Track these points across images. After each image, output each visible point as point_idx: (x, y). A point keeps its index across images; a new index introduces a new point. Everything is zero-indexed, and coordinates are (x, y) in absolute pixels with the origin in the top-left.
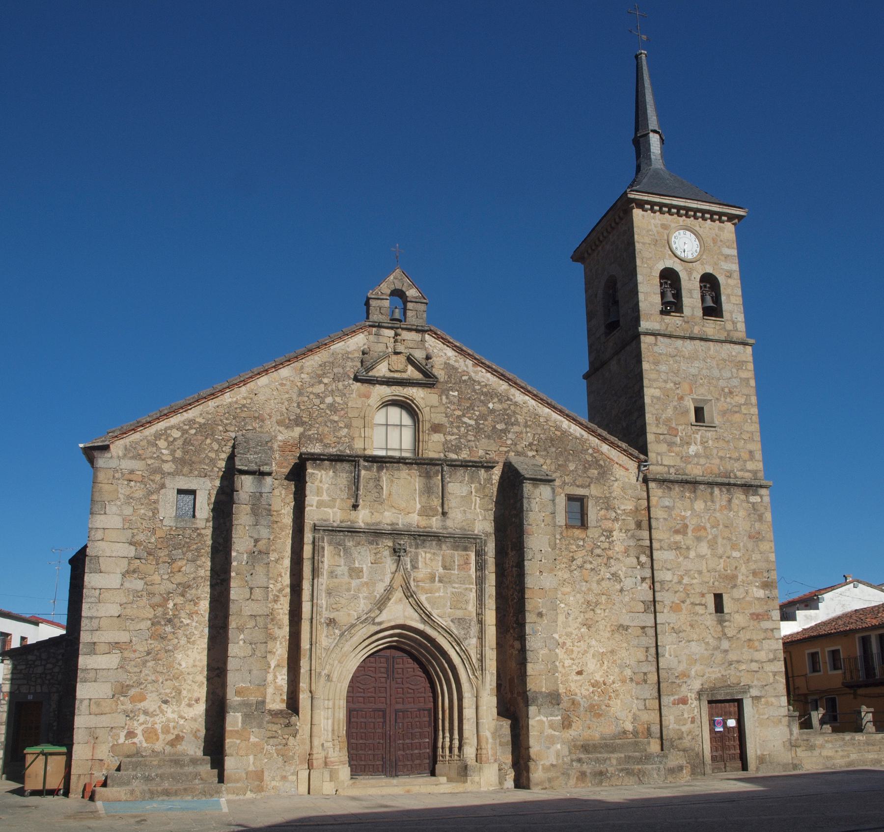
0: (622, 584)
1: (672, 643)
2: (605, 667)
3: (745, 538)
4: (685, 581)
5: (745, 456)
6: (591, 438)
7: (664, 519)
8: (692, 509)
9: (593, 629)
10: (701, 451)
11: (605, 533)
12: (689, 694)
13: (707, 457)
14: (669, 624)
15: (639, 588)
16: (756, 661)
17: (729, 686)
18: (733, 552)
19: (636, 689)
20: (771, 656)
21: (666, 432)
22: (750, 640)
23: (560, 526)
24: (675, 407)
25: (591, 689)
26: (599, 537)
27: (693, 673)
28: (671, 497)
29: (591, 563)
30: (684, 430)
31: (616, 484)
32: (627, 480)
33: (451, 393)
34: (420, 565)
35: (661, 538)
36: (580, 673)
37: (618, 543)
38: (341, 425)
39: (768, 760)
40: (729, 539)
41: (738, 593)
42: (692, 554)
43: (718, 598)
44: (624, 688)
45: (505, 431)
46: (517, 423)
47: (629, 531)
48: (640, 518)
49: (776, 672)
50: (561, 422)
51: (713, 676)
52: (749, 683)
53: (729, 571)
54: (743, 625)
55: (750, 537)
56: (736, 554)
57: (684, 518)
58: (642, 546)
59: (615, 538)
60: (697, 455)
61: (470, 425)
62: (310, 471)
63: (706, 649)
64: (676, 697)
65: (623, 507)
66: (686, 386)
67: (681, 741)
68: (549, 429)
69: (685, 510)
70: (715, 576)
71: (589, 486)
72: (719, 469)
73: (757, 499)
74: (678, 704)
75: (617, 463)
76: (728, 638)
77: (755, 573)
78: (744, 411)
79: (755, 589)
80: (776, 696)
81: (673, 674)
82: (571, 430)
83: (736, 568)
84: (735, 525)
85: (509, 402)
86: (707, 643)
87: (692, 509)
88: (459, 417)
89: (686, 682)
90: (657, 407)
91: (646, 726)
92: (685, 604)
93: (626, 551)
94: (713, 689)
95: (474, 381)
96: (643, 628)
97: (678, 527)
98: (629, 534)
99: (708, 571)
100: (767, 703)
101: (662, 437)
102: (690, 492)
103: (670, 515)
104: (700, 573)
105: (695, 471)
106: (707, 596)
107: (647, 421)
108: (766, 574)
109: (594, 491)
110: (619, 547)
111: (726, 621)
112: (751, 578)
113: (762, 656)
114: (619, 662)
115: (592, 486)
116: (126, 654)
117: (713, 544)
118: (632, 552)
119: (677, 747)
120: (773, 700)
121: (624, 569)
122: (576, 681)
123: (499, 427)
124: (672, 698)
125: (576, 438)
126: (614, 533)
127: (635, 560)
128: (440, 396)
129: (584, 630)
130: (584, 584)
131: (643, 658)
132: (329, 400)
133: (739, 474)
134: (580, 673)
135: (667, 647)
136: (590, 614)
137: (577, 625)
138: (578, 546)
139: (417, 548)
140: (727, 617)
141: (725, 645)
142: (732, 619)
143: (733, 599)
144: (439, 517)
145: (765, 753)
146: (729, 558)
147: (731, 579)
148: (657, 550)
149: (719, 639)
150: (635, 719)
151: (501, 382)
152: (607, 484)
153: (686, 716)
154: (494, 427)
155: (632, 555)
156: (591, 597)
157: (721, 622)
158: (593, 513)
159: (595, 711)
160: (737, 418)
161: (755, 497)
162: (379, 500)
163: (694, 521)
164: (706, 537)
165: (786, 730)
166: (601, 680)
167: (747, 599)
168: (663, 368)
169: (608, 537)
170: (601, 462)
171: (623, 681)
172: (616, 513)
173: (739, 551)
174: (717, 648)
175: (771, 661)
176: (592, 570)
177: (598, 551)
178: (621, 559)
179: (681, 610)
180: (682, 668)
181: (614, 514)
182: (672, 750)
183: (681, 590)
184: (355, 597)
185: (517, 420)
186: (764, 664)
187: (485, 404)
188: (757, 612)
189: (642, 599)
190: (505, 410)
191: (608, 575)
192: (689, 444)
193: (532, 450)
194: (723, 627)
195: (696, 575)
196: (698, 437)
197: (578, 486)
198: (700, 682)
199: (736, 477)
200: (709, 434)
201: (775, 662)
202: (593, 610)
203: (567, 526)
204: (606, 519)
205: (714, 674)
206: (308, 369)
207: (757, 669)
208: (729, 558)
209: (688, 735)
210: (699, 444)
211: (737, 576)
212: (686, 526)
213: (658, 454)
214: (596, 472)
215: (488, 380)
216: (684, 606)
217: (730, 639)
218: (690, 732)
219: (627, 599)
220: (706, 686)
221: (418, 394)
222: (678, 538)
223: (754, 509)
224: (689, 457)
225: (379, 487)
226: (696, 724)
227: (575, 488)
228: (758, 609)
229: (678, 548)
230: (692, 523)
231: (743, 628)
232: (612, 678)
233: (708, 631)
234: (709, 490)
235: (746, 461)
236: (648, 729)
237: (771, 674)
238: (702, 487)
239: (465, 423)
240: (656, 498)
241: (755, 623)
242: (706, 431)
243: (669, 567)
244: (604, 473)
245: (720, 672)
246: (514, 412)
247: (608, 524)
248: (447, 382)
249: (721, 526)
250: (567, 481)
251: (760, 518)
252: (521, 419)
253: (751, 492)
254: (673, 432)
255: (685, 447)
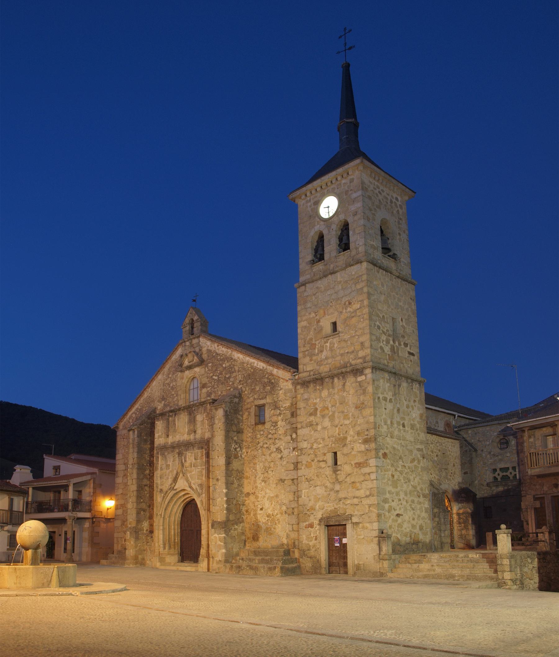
0: (282, 454)
1: (306, 489)
2: (273, 506)
3: (353, 409)
4: (314, 447)
5: (358, 347)
6: (268, 367)
7: (305, 408)
8: (321, 397)
9: (267, 483)
10: (329, 354)
11: (273, 424)
12: (315, 521)
13: (333, 357)
14: (304, 476)
15: (292, 455)
16: (357, 497)
17: (339, 515)
18: (345, 421)
19: (288, 518)
20: (368, 493)
21: (309, 349)
22: (353, 482)
23: (253, 425)
24: (315, 329)
25: (267, 519)
26: (271, 427)
27: (317, 507)
28: (308, 392)
29: (266, 443)
30: (319, 343)
31: (281, 392)
32: (287, 387)
33: (209, 365)
34: (187, 459)
35: (302, 421)
36: (261, 509)
37: (281, 428)
38: (175, 395)
39: (362, 568)
40: (343, 412)
41: (346, 450)
42: (319, 427)
43: (335, 453)
44: (282, 518)
45: (229, 378)
46: (235, 371)
47: (287, 419)
48: (293, 410)
49: (371, 505)
50: (254, 363)
51: (329, 509)
52: (352, 513)
53: (341, 435)
54: (349, 472)
55: (356, 408)
56: (347, 422)
57: (315, 404)
58: (293, 428)
59: (279, 426)
60: (327, 358)
61: (216, 380)
62: (156, 422)
63: (325, 491)
64: (307, 523)
65: (284, 406)
66: (321, 312)
67: (309, 551)
68: (248, 369)
69: (316, 399)
70: (333, 440)
71: (266, 397)
72: (340, 363)
73: (363, 377)
74: (308, 528)
75: (282, 378)
76: (339, 482)
77: (358, 434)
78: (358, 314)
79: (358, 445)
80: (370, 522)
81: (306, 508)
82: (258, 367)
83: (346, 432)
84: (346, 401)
85: (231, 361)
86: (326, 487)
87: (321, 397)
88: (212, 376)
89: (313, 513)
90: (305, 333)
91: (293, 541)
92: (315, 461)
93: (285, 434)
94: (328, 518)
95: (218, 354)
96: (293, 480)
97: (311, 411)
98: (287, 422)
99: (329, 438)
100: (363, 527)
101: (307, 353)
102: (320, 386)
103: (307, 405)
104: (323, 439)
105: (324, 369)
106: (327, 454)
107: (299, 345)
108: (366, 433)
109: (269, 400)
110: (281, 431)
111: (338, 471)
112: (356, 437)
113: (361, 493)
114: (280, 502)
115: (267, 397)
116: (124, 509)
117: (332, 418)
118: (289, 433)
119: (307, 555)
120: (368, 525)
121: (284, 444)
122: (260, 514)
123: (227, 376)
124: (305, 524)
125: (261, 370)
126: (279, 423)
127: (289, 438)
128: (205, 368)
129: (263, 484)
130: (263, 457)
131: (292, 499)
132: (171, 385)
133: (353, 362)
134: (261, 509)
135: (303, 491)
136: (266, 475)
137: (260, 481)
138: (261, 435)
139: (186, 451)
140: (339, 468)
141: (337, 487)
142: (342, 469)
143: (343, 454)
144: (193, 434)
145: (360, 563)
146: (341, 425)
147: (342, 441)
148: (300, 429)
149: (334, 483)
150: (287, 537)
151: (229, 350)
152: (276, 393)
153: (312, 535)
154: (225, 377)
155: (288, 434)
156: (267, 464)
157: (335, 471)
158: (268, 413)
159: (269, 532)
160: (354, 320)
161: (361, 377)
162: (175, 431)
163: (321, 405)
164: (328, 414)
165: (376, 547)
166: (271, 513)
167: (353, 453)
168: (309, 305)
169: (274, 426)
170: (273, 381)
171: (282, 514)
172: (280, 410)
173: (349, 419)
174: (332, 490)
175: (367, 497)
176: (267, 447)
177: (270, 436)
178: (282, 438)
179: (312, 466)
180: (311, 504)
181: (278, 411)
182: (304, 557)
183: (312, 453)
184: (168, 478)
185: (235, 370)
186: (362, 499)
187: (221, 365)
188: (359, 461)
189: (293, 462)
190: (230, 365)
191: (275, 450)
192: (322, 351)
193: (240, 384)
194: (337, 475)
195: (321, 442)
196: (328, 344)
197: (260, 399)
198: (321, 513)
199: (351, 365)
200: (335, 340)
201: (370, 497)
202: (267, 472)
203: (256, 424)
204: (274, 415)
205: (330, 507)
206: (165, 373)
207: (358, 503)
208: (341, 425)
209: (313, 548)
210: (328, 349)
211: (346, 438)
212: (316, 409)
213: (304, 365)
214: (269, 388)
215: (223, 351)
216: (313, 463)
217: (340, 483)
218: (314, 546)
219: (285, 463)
220: (324, 516)
221: (197, 369)
222: (312, 418)
223: (360, 386)
224: (322, 361)
225: (175, 424)
226: (317, 541)
227: (259, 401)
228: (360, 459)
229: (311, 425)
230: (319, 407)
231: (349, 475)
232: (276, 512)
233: (327, 479)
234: (331, 380)
235: (358, 351)
236: (294, 543)
237: (367, 506)
238: (327, 380)
239: (214, 379)
240: (300, 395)
241: (358, 469)
242: (333, 338)
243: (306, 439)
244: (273, 387)
245: (333, 506)
246: (234, 365)
247: (275, 419)
248: (207, 360)
249: (338, 404)
250: (256, 397)
251: (364, 392)
252: (237, 368)
253: (359, 373)
254: (313, 346)
255: (320, 355)
